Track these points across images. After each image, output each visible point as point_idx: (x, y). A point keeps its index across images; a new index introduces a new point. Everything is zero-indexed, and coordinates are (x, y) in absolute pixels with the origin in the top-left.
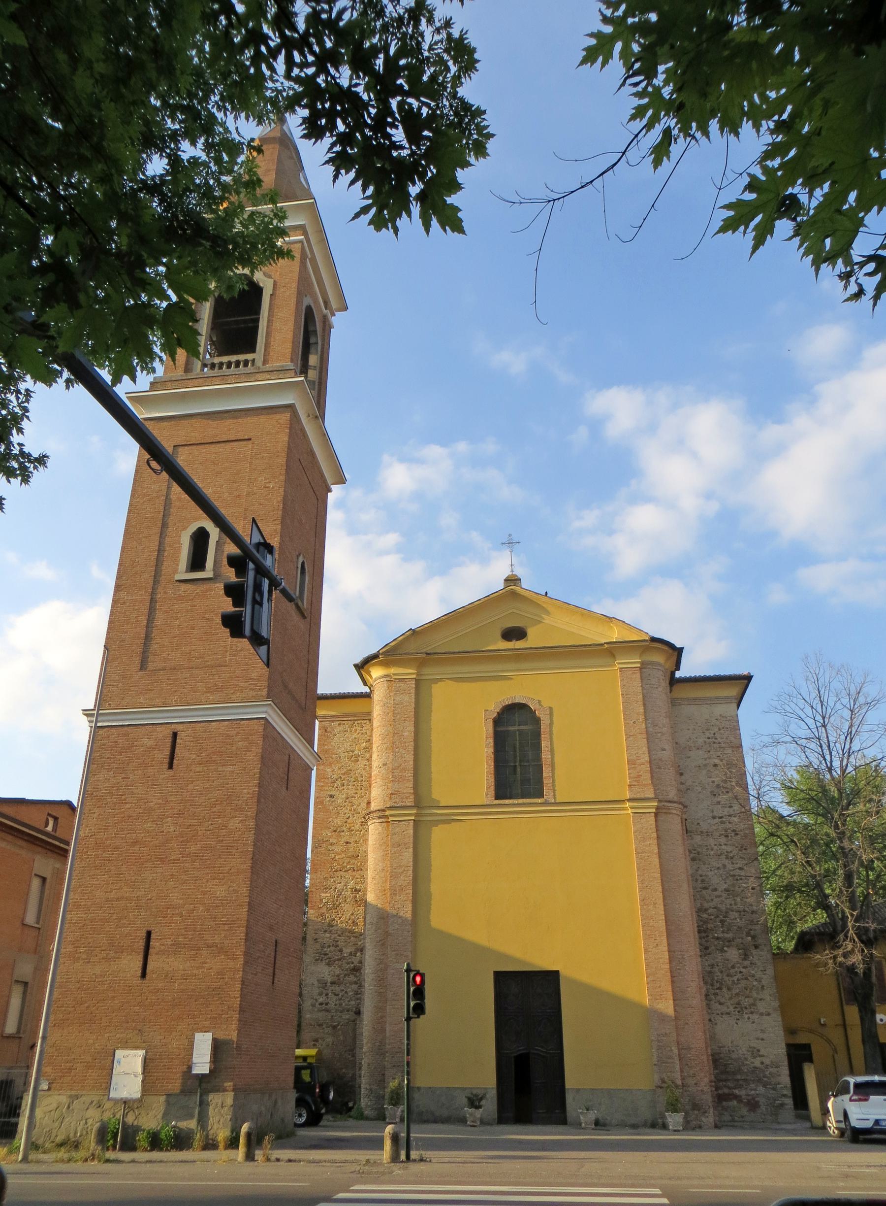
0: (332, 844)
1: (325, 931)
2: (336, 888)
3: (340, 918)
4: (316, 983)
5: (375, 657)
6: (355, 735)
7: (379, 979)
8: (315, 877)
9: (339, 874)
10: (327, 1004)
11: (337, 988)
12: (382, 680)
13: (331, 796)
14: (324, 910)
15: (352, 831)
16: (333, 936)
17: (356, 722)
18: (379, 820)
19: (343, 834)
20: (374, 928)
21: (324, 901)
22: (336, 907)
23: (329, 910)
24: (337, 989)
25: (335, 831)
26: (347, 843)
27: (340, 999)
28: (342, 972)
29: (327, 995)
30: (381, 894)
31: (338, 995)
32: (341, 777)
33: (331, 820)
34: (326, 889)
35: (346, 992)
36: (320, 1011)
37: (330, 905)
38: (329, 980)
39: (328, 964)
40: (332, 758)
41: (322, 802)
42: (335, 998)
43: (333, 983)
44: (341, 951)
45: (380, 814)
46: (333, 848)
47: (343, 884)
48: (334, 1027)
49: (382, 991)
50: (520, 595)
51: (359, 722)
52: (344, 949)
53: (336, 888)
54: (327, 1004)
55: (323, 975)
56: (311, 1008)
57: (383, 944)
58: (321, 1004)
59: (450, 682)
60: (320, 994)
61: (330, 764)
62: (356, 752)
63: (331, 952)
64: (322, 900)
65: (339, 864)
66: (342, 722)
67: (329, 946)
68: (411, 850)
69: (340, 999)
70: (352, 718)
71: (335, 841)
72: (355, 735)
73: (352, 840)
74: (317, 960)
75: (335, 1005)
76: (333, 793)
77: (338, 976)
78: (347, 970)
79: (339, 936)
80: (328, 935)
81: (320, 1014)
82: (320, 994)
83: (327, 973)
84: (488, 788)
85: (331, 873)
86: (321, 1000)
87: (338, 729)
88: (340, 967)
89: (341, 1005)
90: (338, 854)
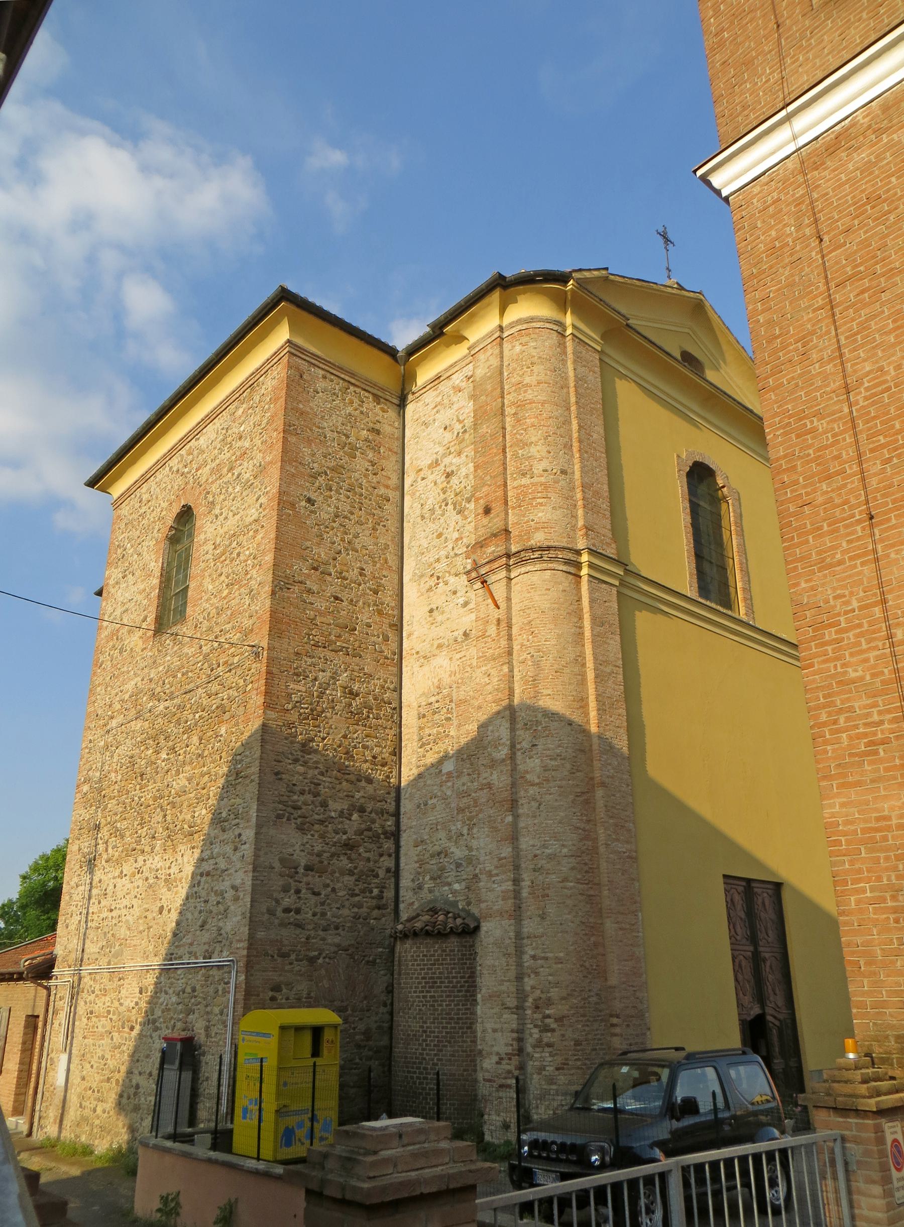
0: (309, 591)
1: (296, 761)
2: (316, 679)
3: (324, 739)
4: (277, 865)
5: (562, 278)
6: (349, 409)
7: (586, 868)
8: (277, 645)
9: (320, 652)
10: (298, 911)
11: (317, 879)
12: (548, 325)
13: (309, 501)
14: (294, 717)
15: (345, 579)
16: (311, 773)
17: (352, 388)
18: (565, 568)
19: (328, 578)
20: (568, 766)
21: (295, 698)
22: (315, 715)
23: (303, 718)
24: (316, 880)
25: (316, 569)
26: (336, 598)
27: (323, 904)
28: (326, 848)
29: (298, 891)
30: (576, 705)
31: (319, 894)
32: (326, 474)
33: (308, 544)
34: (298, 675)
35: (334, 890)
36: (283, 925)
37: (305, 709)
38: (303, 863)
39: (301, 829)
40: (311, 430)
41: (293, 505)
42: (313, 899)
43: (308, 868)
44: (324, 804)
45: (570, 556)
46: (311, 599)
47: (328, 674)
48: (312, 960)
49: (592, 893)
50: (706, 313)
51: (358, 390)
52: (330, 802)
53: (316, 679)
54: (298, 911)
55: (290, 850)
56: (266, 916)
57: (587, 802)
58: (287, 910)
59: (633, 384)
60: (285, 889)
61: (309, 441)
62: (352, 439)
63: (305, 803)
64: (289, 695)
65: (322, 635)
66: (328, 375)
67: (302, 793)
68: (618, 638)
69: (323, 904)
70: (347, 378)
71: (315, 588)
72: (349, 409)
73: (344, 595)
74: (279, 817)
75: (314, 915)
76: (313, 496)
77: (319, 855)
78: (334, 845)
79: (322, 774)
80: (301, 769)
81: (284, 932)
82: (285, 889)
83: (297, 847)
84: (691, 574)
85: (307, 647)
86: (287, 902)
87: (321, 385)
88: (322, 836)
89: (323, 914)
90: (321, 614)
